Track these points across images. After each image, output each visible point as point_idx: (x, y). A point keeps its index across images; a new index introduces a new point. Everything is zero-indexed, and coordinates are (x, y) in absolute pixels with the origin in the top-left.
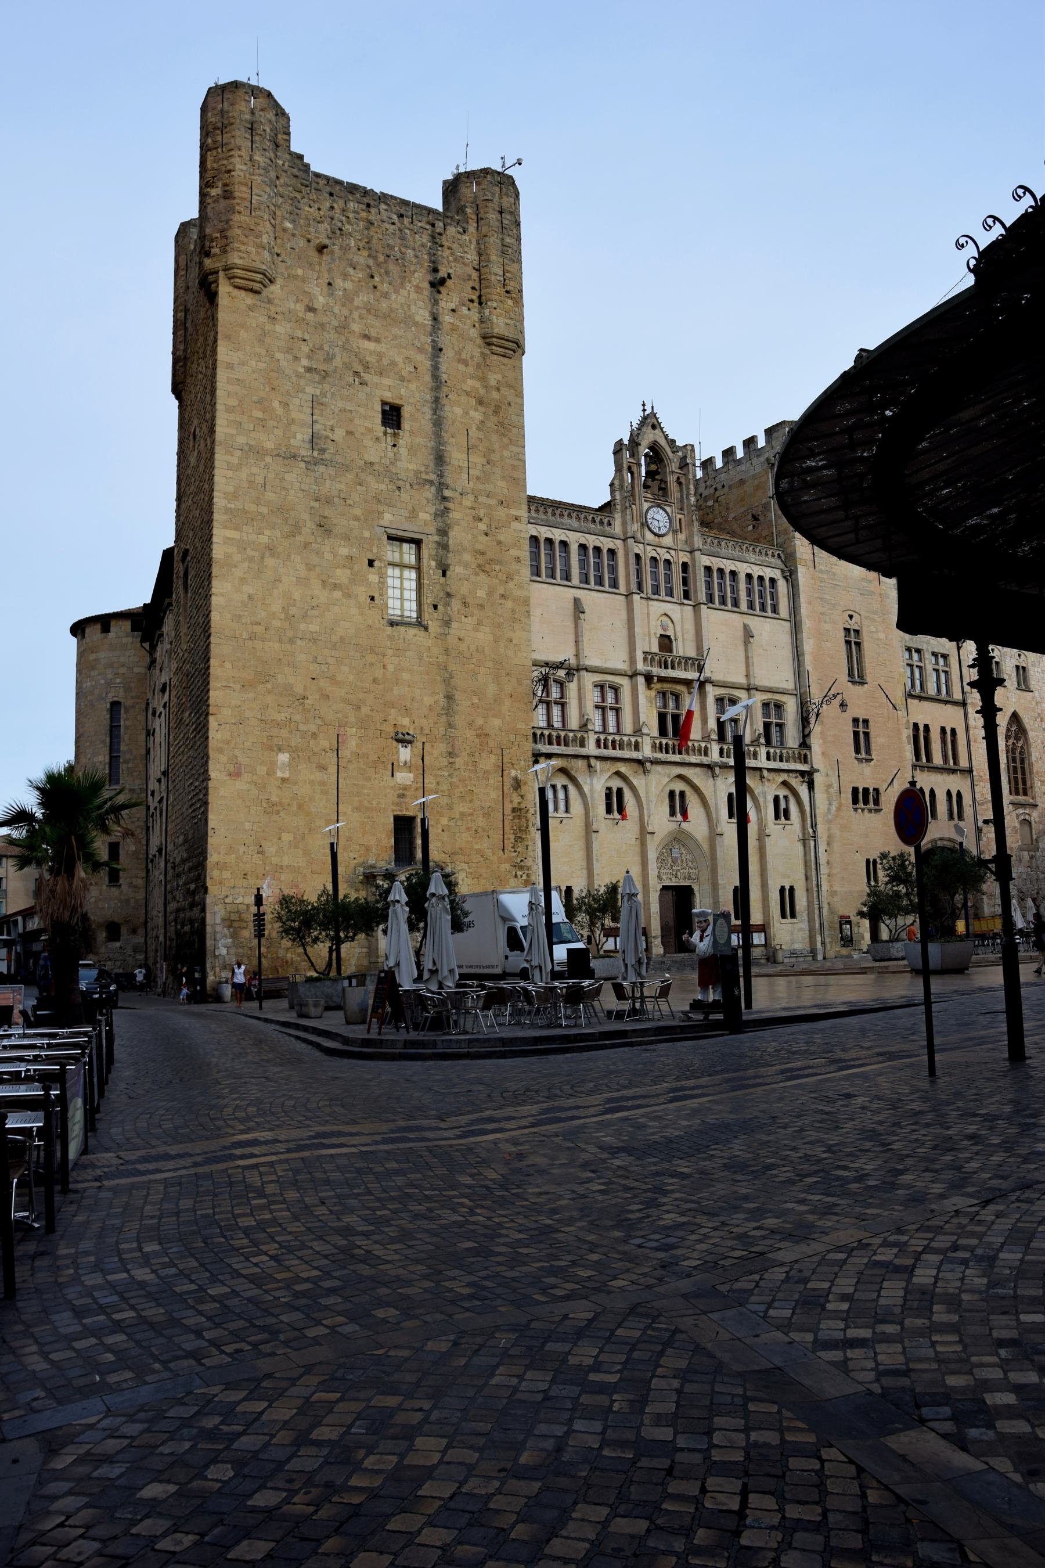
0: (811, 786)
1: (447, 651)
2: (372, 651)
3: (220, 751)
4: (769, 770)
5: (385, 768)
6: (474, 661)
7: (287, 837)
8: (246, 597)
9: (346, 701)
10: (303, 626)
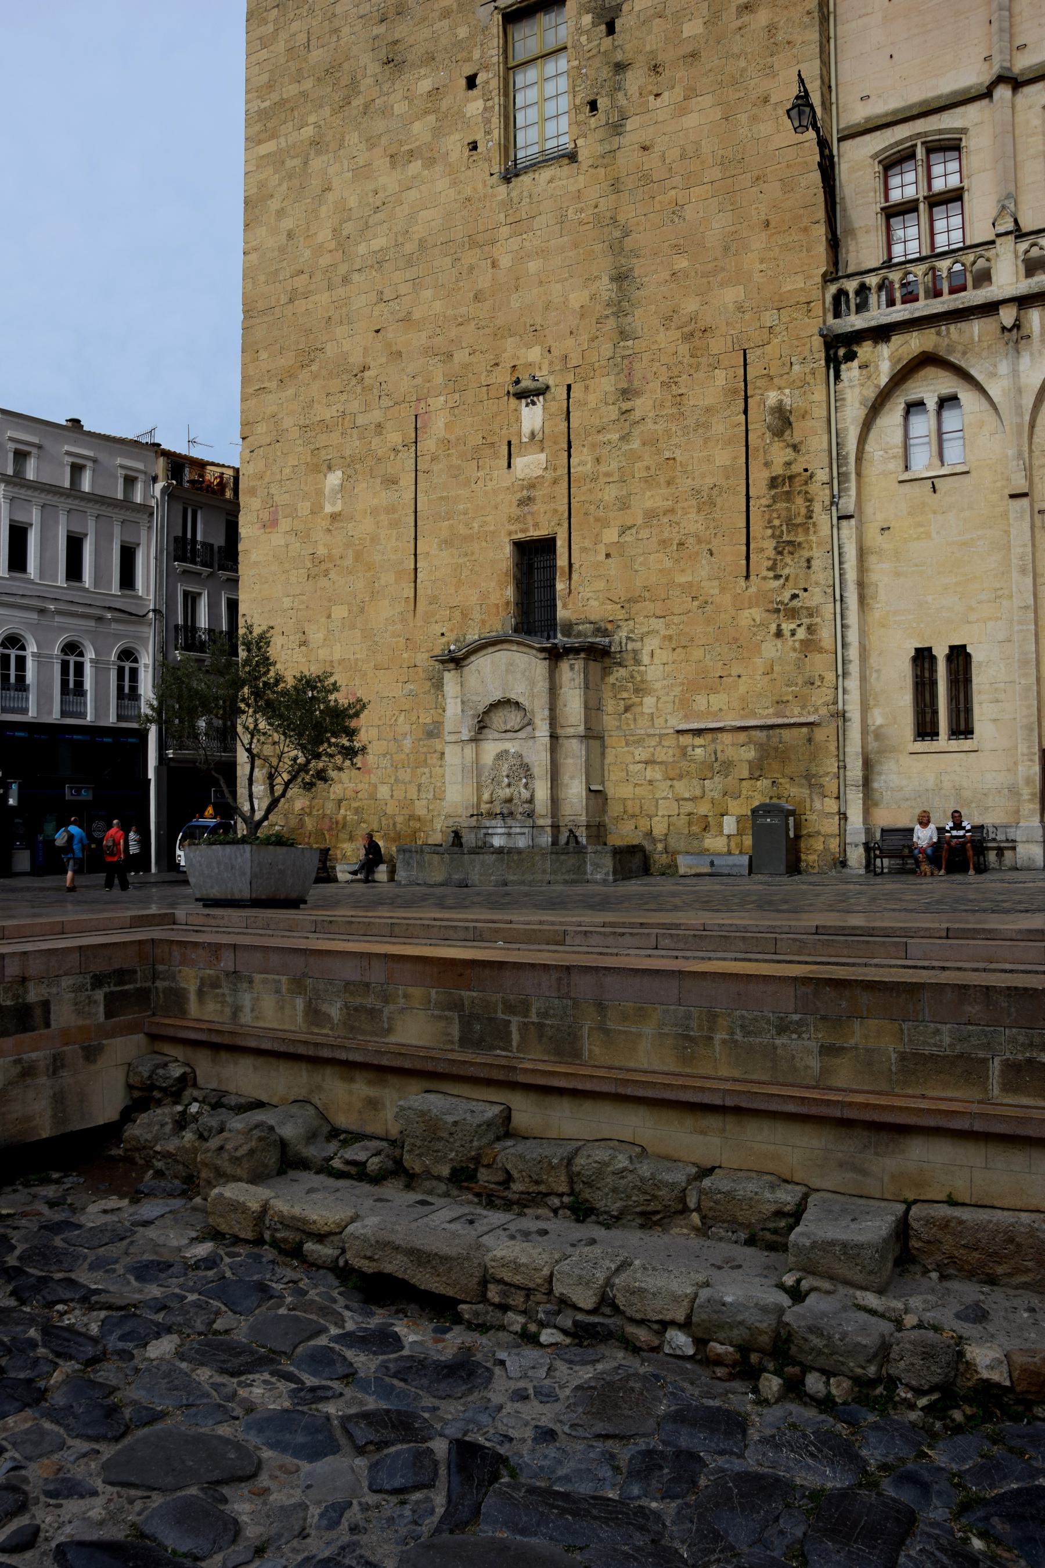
1: (616, 186)
2: (473, 244)
3: (253, 492)
5: (496, 456)
6: (677, 180)
7: (340, 612)
8: (284, 237)
9: (429, 351)
10: (362, 249)
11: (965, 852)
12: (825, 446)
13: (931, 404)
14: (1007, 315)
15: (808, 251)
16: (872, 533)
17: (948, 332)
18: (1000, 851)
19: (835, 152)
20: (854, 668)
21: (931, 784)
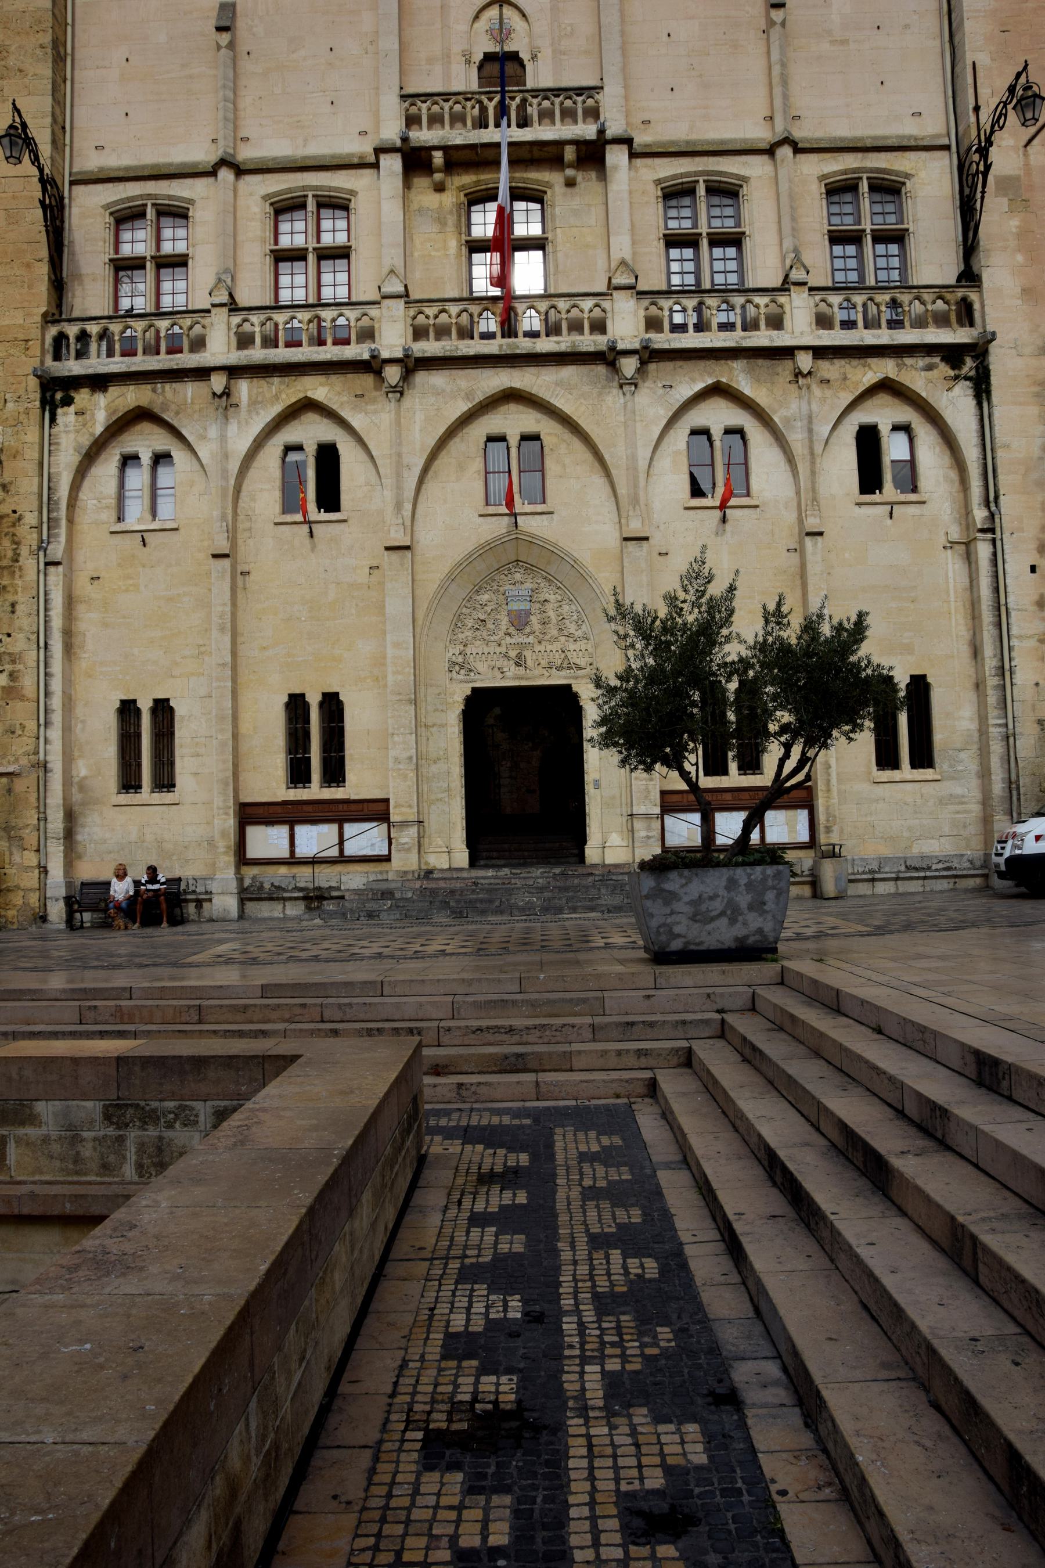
0: (982, 387)
4: (820, 352)
11: (163, 904)
12: (35, 489)
13: (146, 458)
14: (218, 382)
15: (30, 287)
16: (82, 583)
17: (163, 391)
18: (199, 903)
19: (66, 194)
20: (57, 718)
21: (134, 837)
